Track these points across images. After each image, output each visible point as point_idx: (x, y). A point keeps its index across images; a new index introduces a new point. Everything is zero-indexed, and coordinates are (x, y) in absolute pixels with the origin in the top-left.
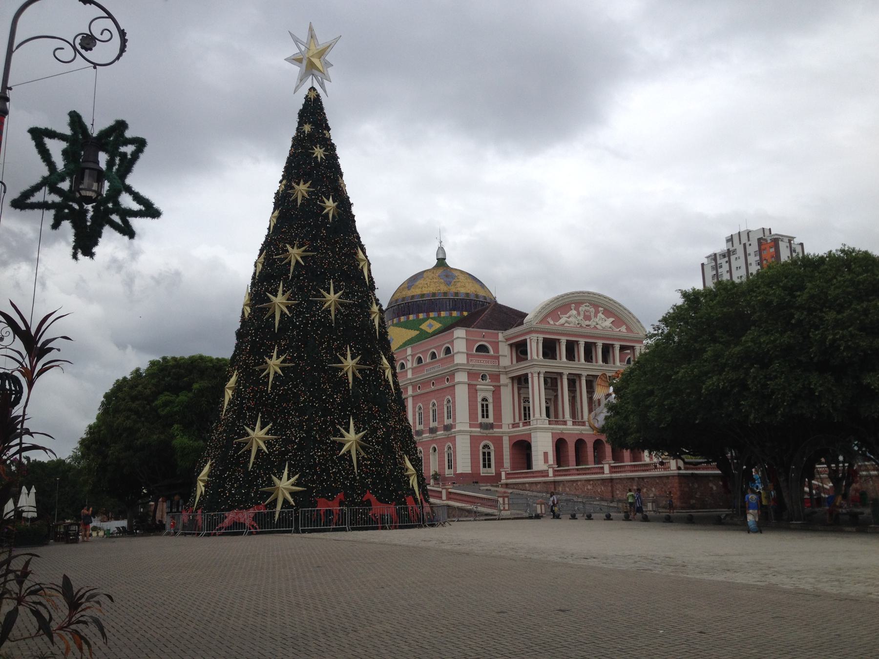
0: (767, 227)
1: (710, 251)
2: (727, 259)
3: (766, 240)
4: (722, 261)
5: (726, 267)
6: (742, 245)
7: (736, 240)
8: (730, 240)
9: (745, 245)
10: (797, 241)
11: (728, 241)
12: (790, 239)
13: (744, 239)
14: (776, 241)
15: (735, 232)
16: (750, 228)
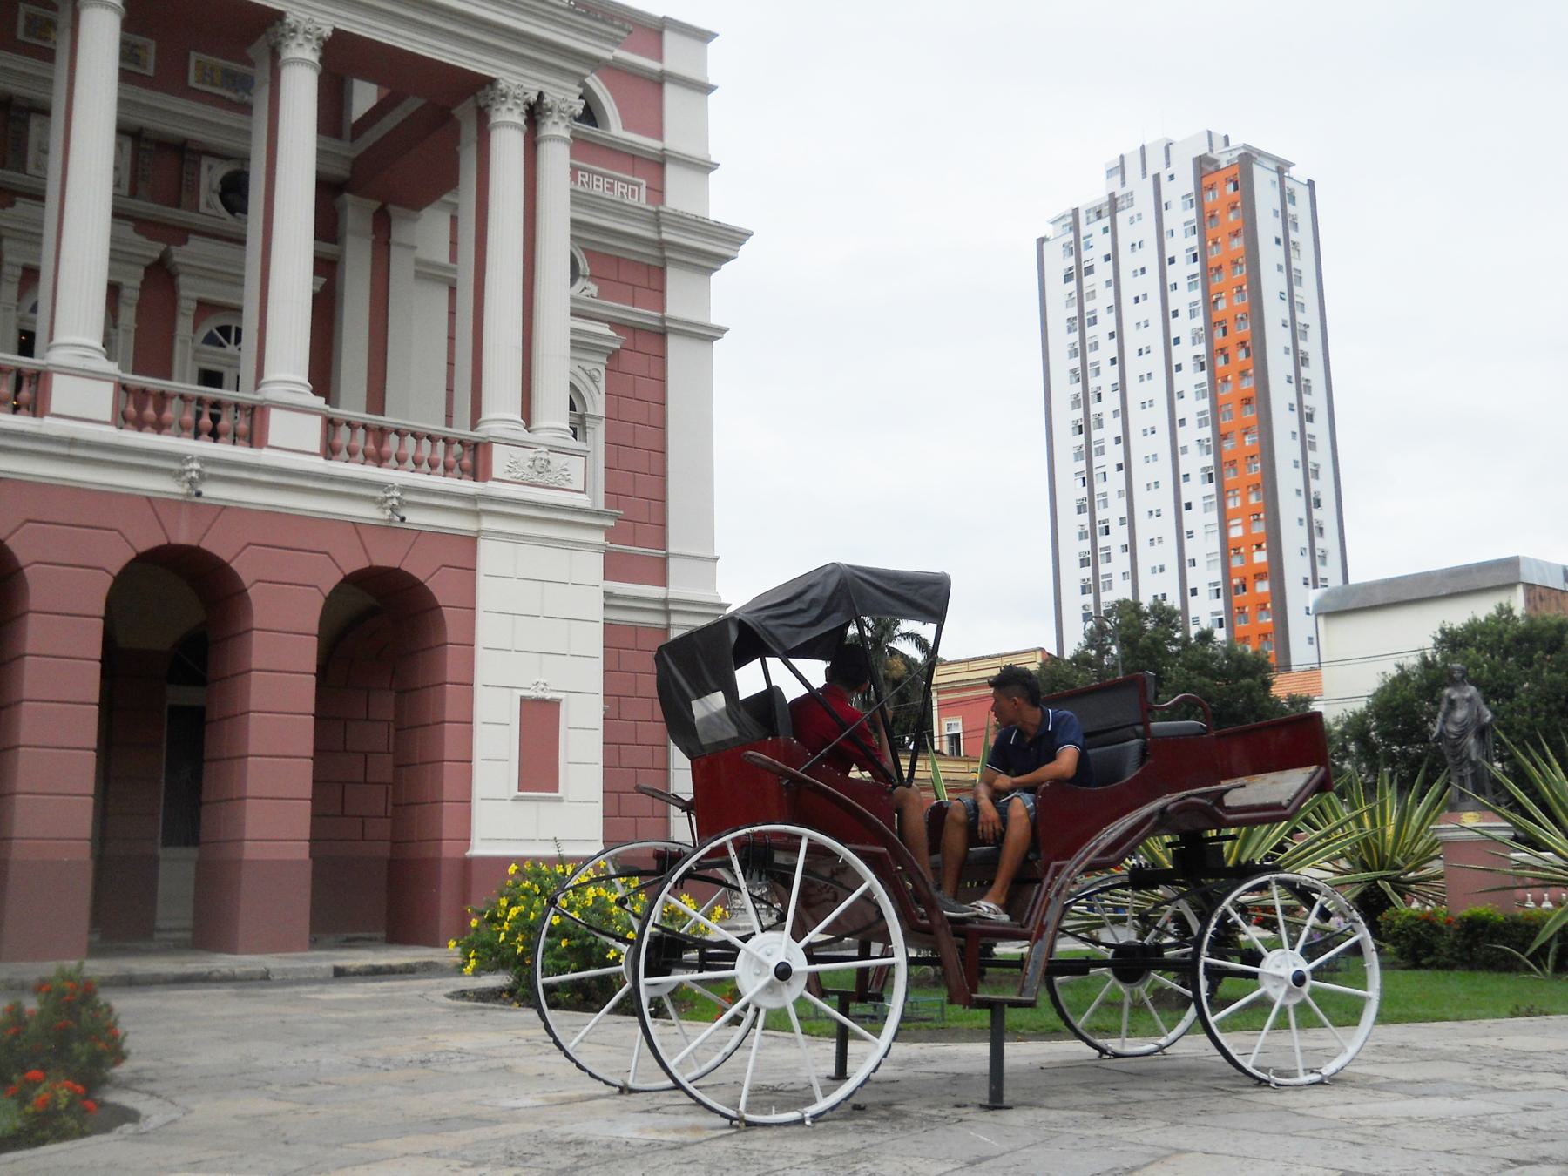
0: (1219, 132)
1: (1066, 208)
2: (1106, 222)
3: (1214, 161)
4: (1094, 230)
5: (1103, 245)
6: (1149, 180)
7: (1133, 168)
8: (1121, 168)
9: (1157, 177)
10: (1298, 173)
11: (1110, 173)
12: (1282, 168)
13: (1156, 164)
14: (1248, 158)
15: (1130, 148)
16: (1173, 138)
